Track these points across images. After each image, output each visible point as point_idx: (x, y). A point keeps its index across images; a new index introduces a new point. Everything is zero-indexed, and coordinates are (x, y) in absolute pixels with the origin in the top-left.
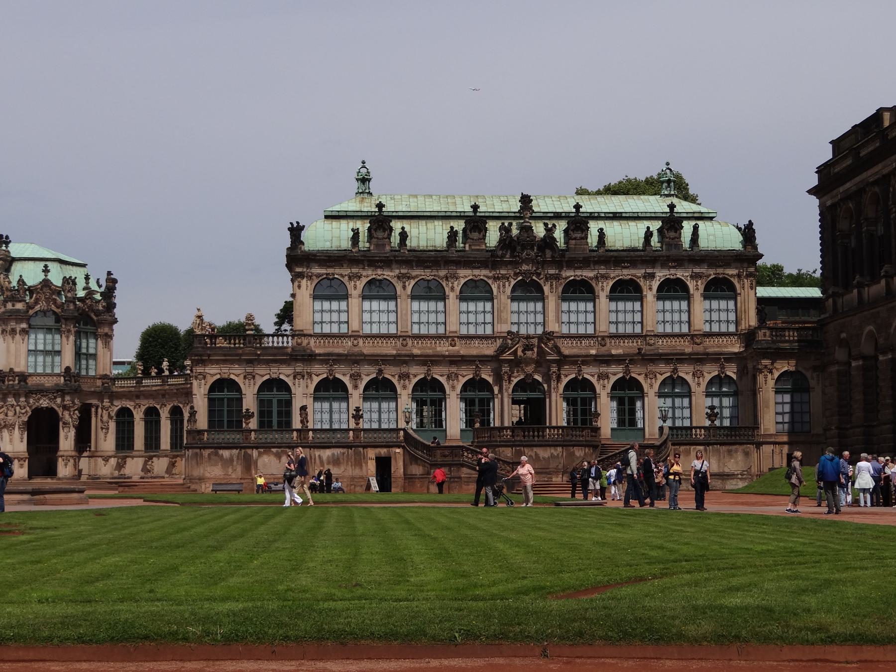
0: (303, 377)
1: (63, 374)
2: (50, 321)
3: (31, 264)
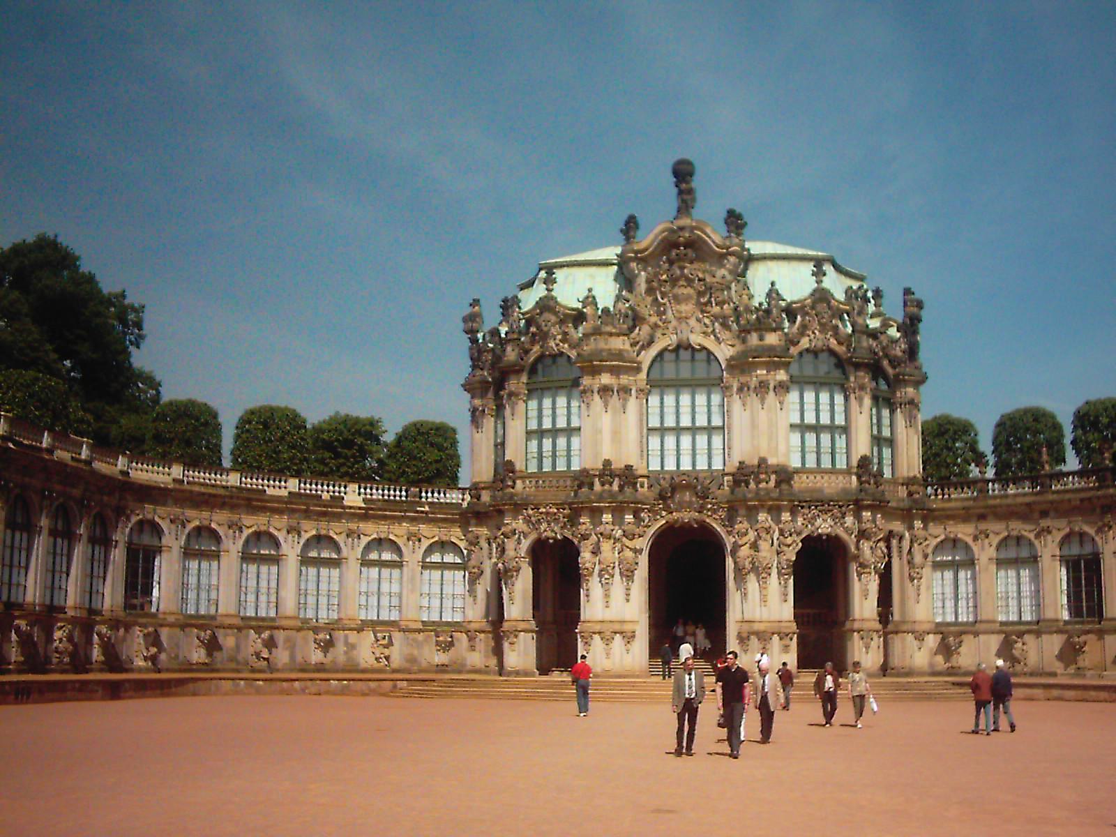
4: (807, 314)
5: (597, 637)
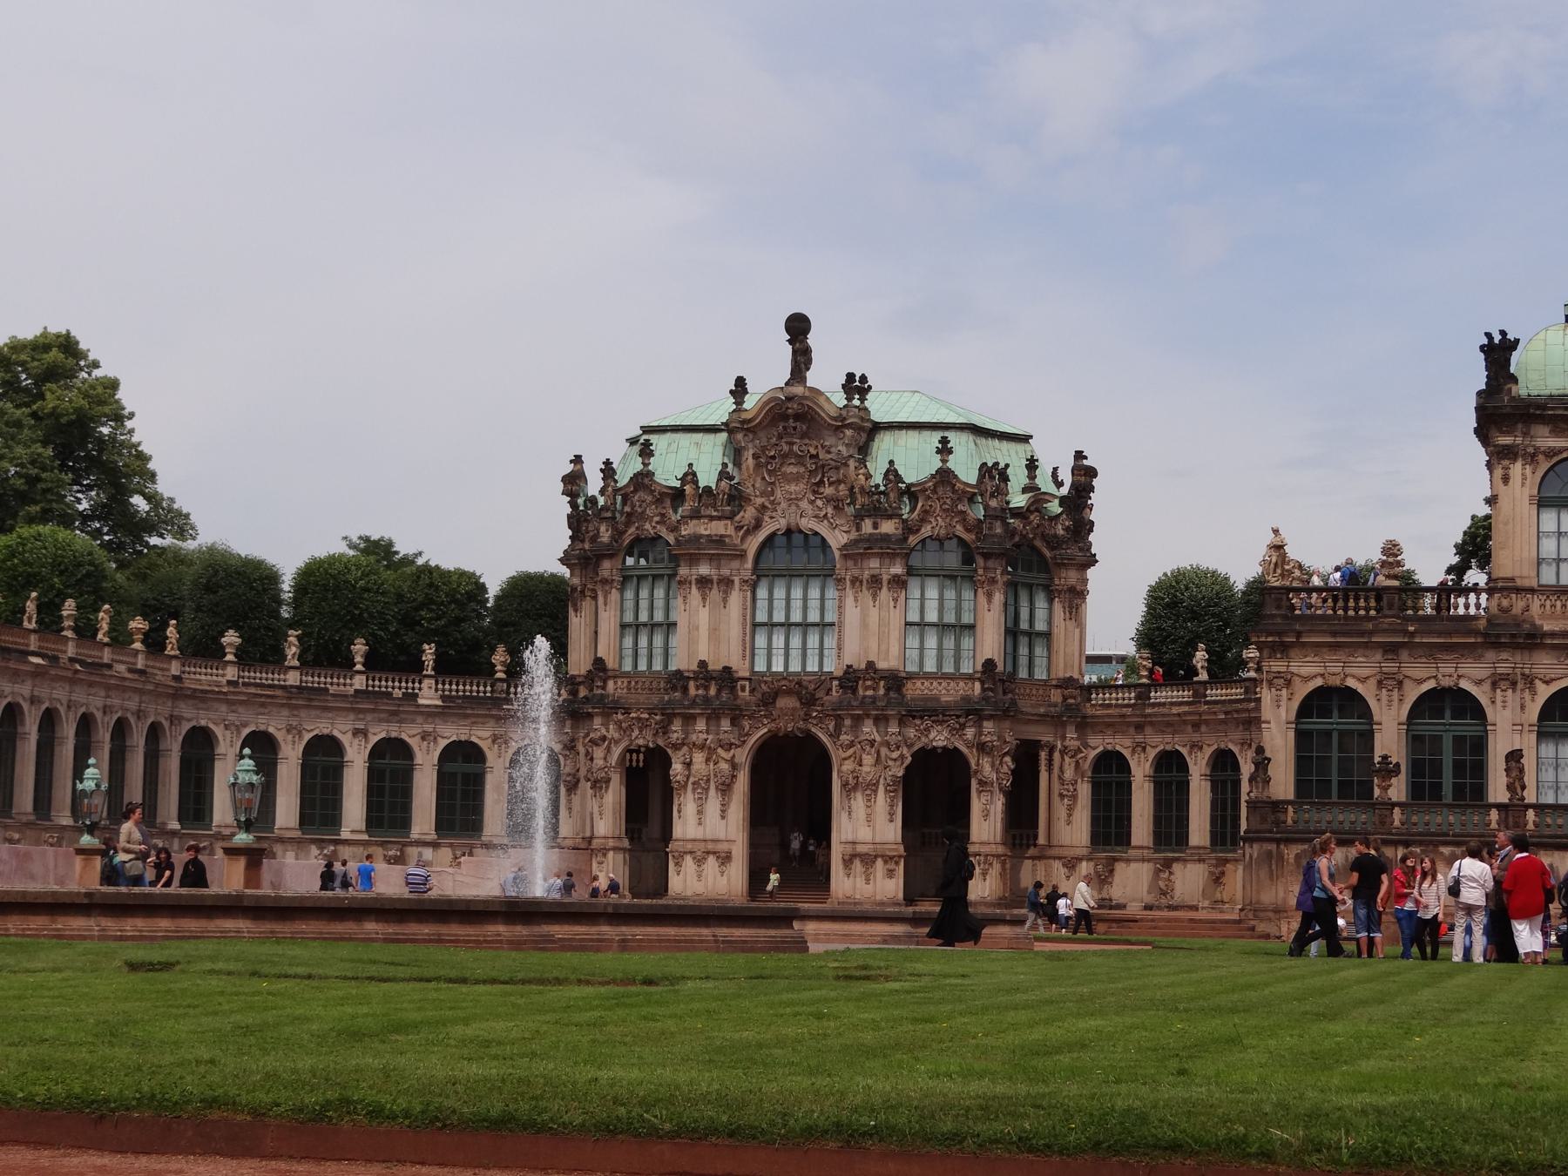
0: (1514, 684)
1: (978, 675)
2: (953, 560)
3: (912, 438)
4: (929, 498)
5: (688, 859)
